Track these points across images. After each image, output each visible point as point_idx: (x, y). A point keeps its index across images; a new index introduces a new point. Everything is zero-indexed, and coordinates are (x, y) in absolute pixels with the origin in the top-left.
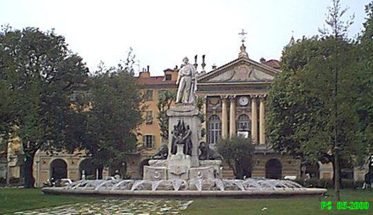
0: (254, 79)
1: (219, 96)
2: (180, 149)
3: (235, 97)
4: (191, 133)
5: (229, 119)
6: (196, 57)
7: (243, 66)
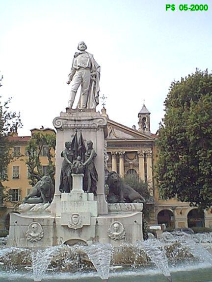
2: (78, 182)
4: (95, 155)
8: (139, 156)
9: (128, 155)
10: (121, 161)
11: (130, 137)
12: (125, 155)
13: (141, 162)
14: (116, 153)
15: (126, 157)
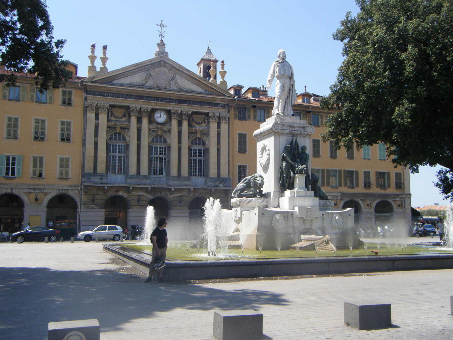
0: (175, 88)
1: (127, 108)
3: (150, 109)
5: (139, 139)
6: (93, 46)
7: (162, 69)
8: (211, 120)
9: (194, 116)
10: (185, 124)
11: (200, 90)
12: (191, 117)
13: (213, 126)
14: (179, 112)
15: (191, 120)
